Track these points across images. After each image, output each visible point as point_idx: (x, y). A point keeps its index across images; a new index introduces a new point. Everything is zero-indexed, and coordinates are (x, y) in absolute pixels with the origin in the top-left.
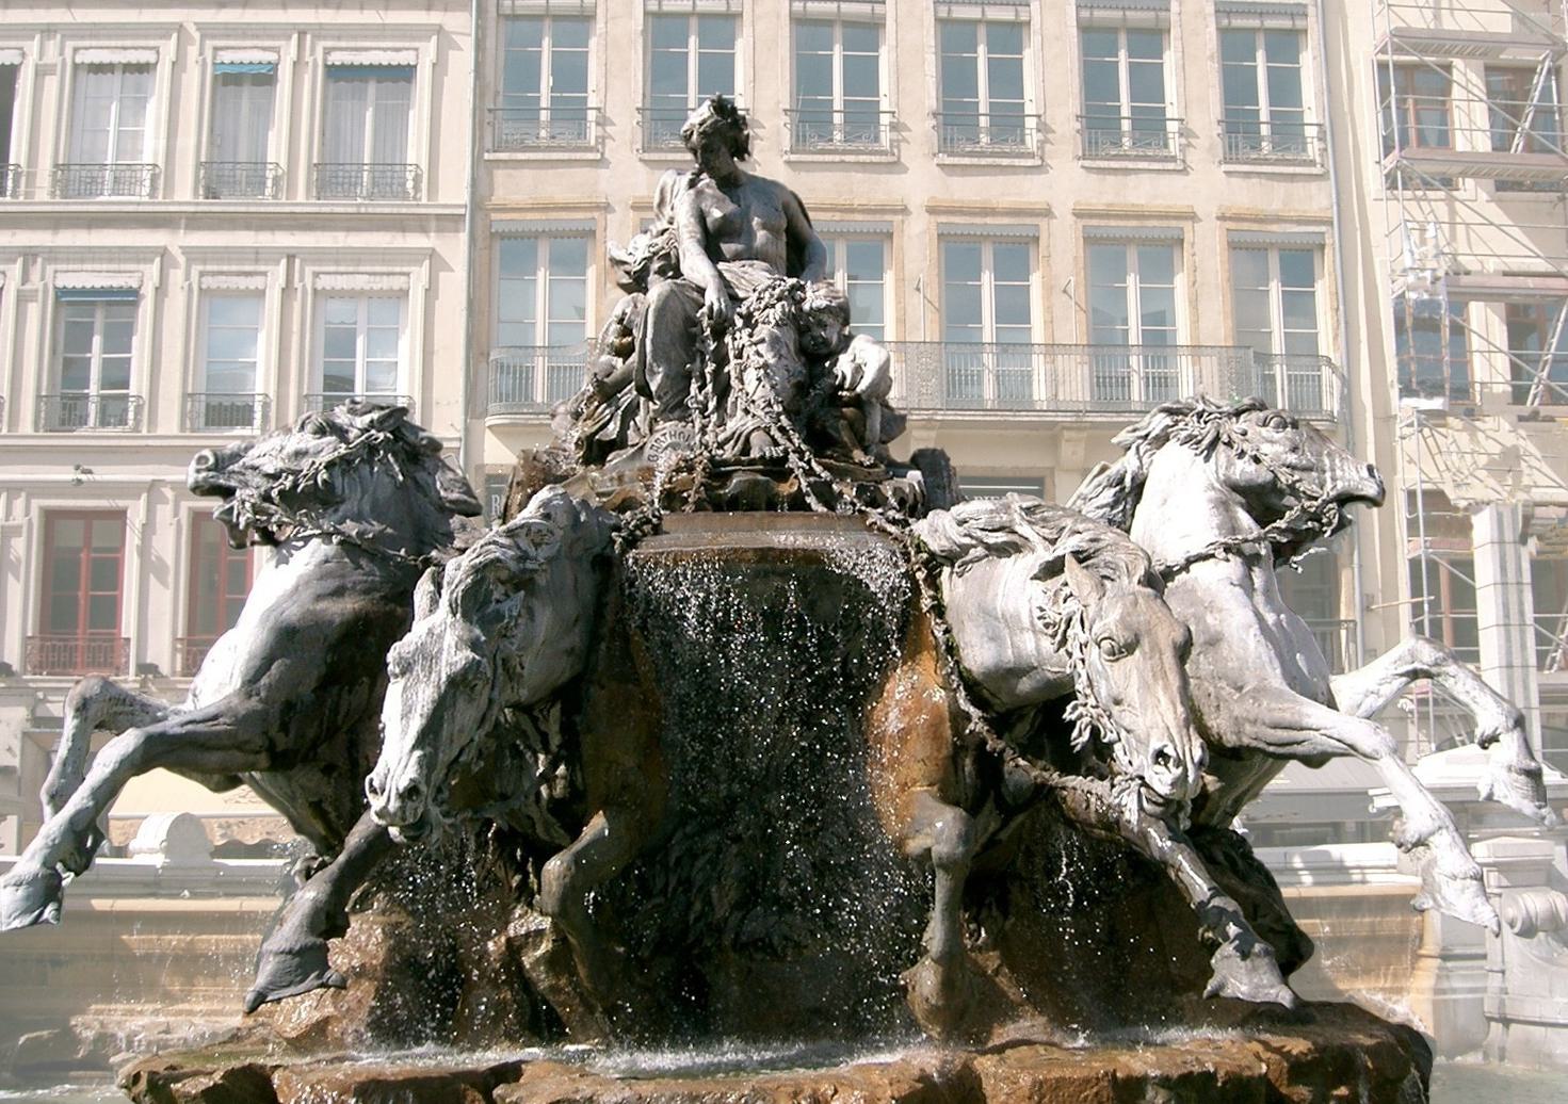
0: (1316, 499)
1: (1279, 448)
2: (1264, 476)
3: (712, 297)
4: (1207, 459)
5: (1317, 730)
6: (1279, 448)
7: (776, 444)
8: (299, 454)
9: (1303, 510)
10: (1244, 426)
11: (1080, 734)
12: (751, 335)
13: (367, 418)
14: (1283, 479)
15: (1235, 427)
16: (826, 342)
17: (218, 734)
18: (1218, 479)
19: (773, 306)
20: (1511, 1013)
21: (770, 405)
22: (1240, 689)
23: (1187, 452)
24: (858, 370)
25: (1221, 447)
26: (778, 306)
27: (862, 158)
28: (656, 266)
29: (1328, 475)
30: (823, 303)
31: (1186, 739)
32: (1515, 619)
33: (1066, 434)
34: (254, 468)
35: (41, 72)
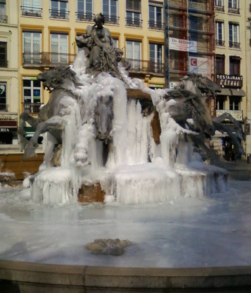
2: (205, 87)
8: (56, 74)
28: (90, 42)
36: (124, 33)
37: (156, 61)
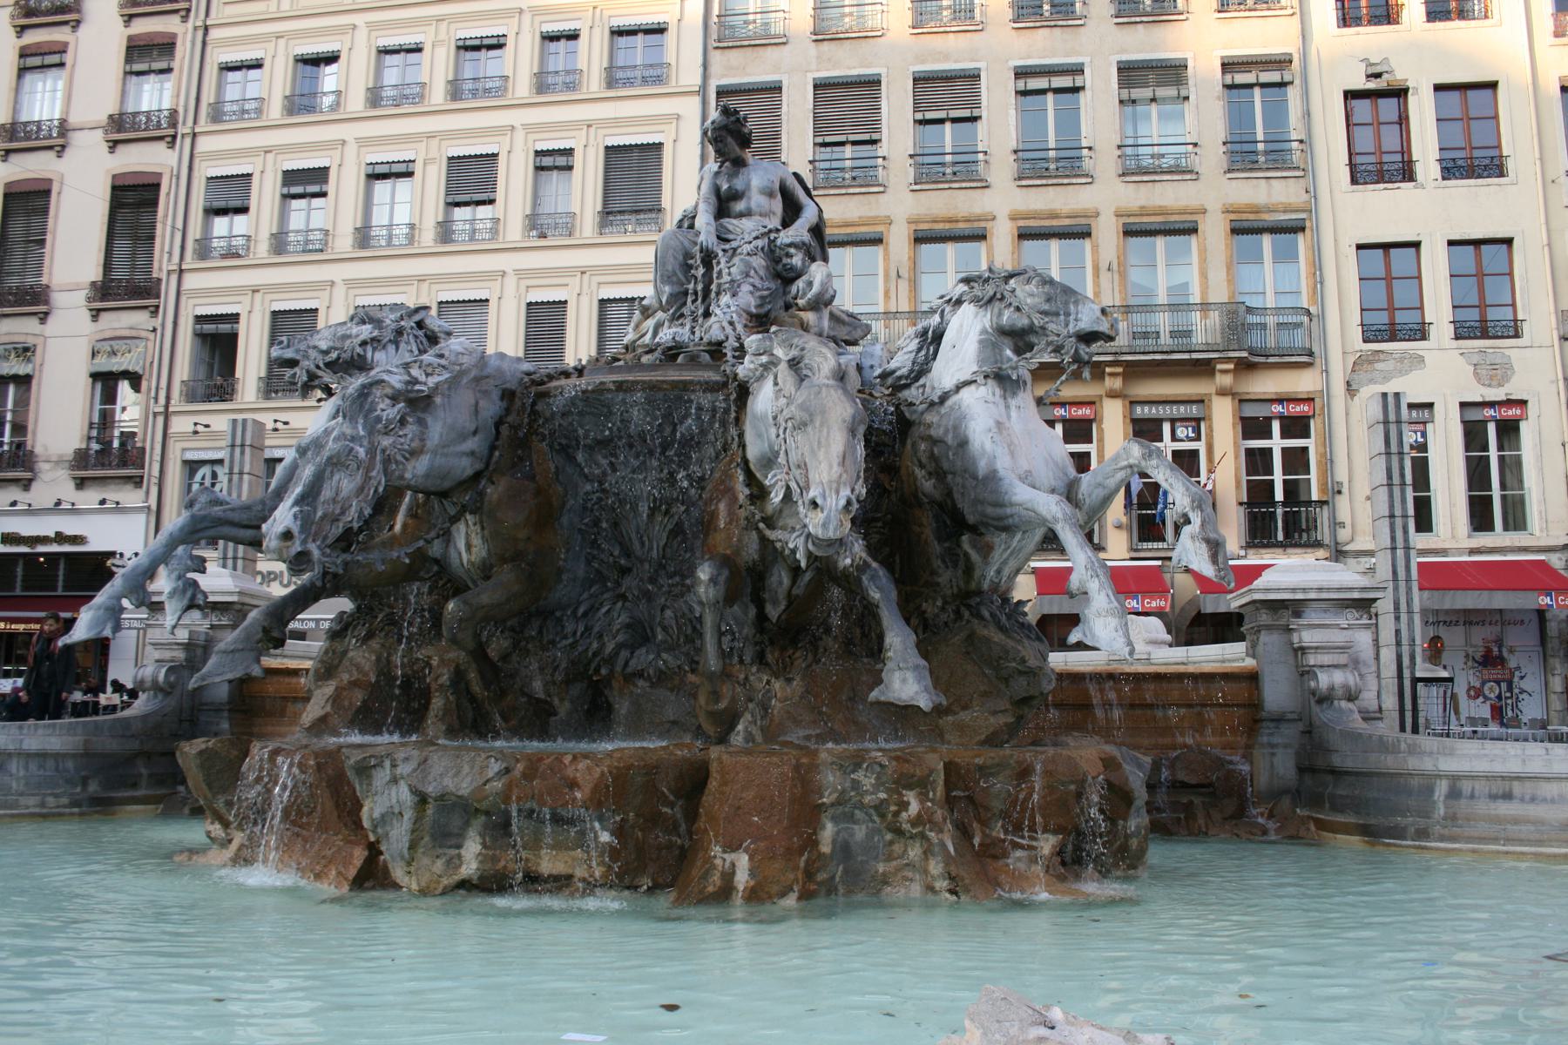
1: (1037, 300)
2: (1024, 322)
6: (1037, 300)
14: (1036, 322)
16: (792, 268)
18: (992, 327)
24: (810, 284)
27: (964, 185)
29: (1072, 317)
32: (1396, 479)
33: (1108, 370)
34: (315, 347)
36: (1113, 209)
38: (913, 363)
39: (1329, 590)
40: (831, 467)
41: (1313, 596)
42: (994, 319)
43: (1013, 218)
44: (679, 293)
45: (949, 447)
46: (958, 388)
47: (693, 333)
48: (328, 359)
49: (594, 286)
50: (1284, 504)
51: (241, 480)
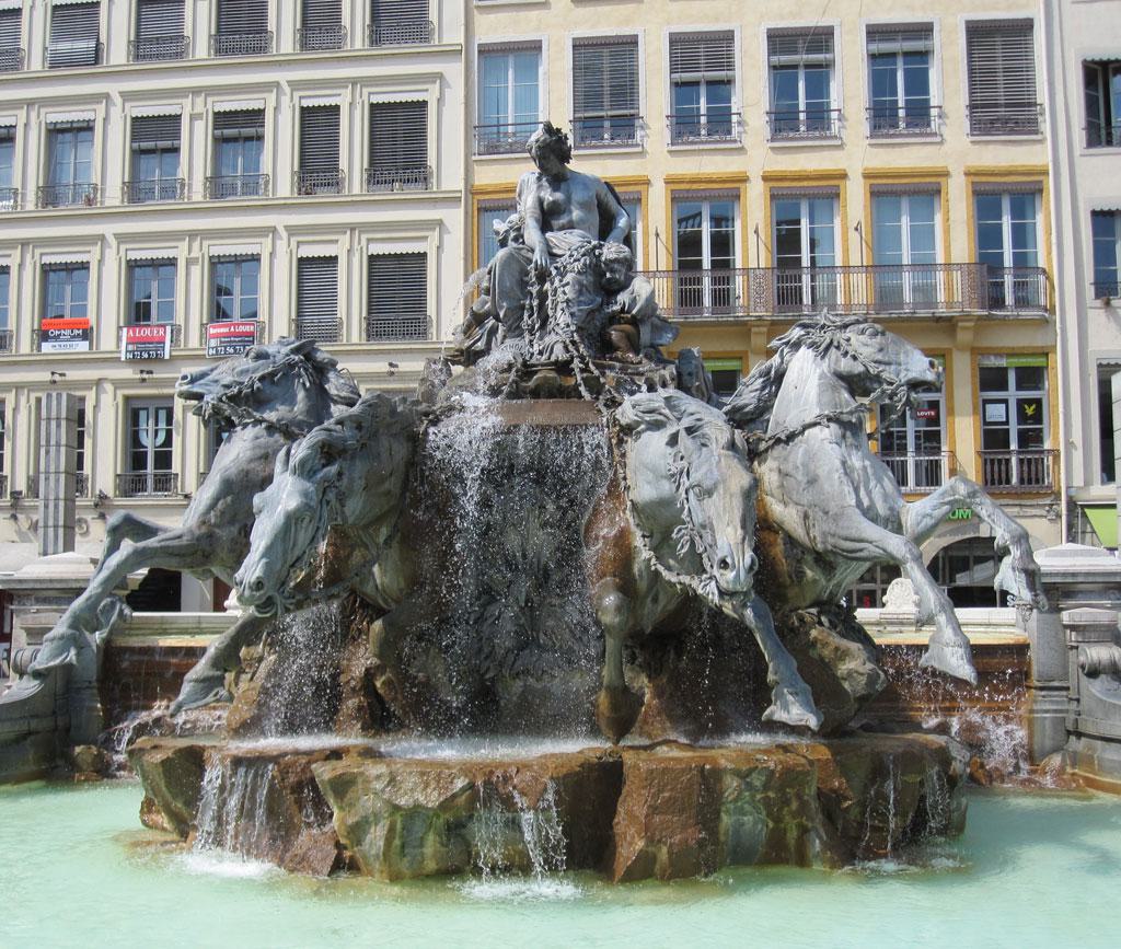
0: (892, 384)
2: (858, 368)
3: (537, 257)
4: (823, 358)
5: (871, 543)
7: (567, 351)
8: (242, 373)
9: (883, 392)
10: (849, 335)
11: (682, 546)
12: (561, 281)
13: (289, 347)
14: (871, 371)
15: (840, 336)
16: (617, 281)
17: (180, 547)
18: (829, 372)
19: (579, 260)
20: (1082, 728)
21: (568, 326)
22: (826, 513)
23: (810, 353)
24: (634, 301)
25: (833, 350)
26: (582, 260)
28: (513, 234)
30: (614, 256)
31: (740, 553)
34: (216, 381)
35: (193, 118)
36: (861, 171)
37: (1008, 261)
38: (759, 400)
39: (1094, 574)
40: (736, 531)
41: (1080, 579)
42: (832, 365)
43: (765, 179)
44: (516, 307)
45: (799, 483)
46: (806, 427)
47: (532, 346)
48: (229, 392)
49: (364, 243)
50: (1019, 453)
51: (58, 451)
